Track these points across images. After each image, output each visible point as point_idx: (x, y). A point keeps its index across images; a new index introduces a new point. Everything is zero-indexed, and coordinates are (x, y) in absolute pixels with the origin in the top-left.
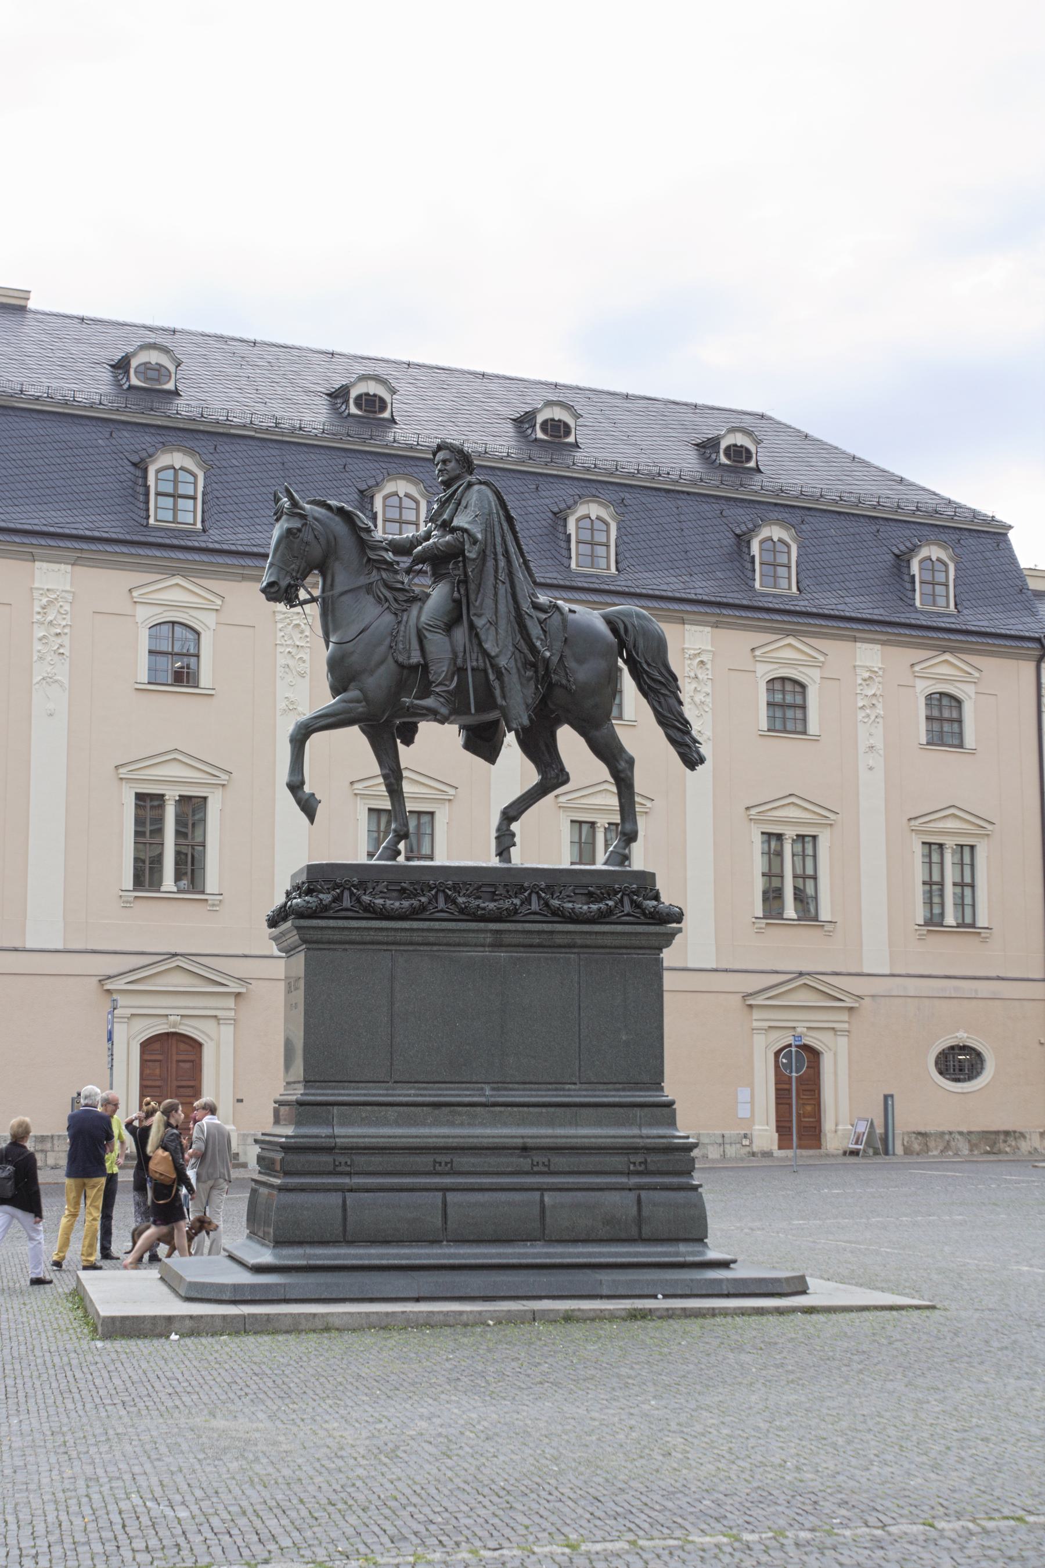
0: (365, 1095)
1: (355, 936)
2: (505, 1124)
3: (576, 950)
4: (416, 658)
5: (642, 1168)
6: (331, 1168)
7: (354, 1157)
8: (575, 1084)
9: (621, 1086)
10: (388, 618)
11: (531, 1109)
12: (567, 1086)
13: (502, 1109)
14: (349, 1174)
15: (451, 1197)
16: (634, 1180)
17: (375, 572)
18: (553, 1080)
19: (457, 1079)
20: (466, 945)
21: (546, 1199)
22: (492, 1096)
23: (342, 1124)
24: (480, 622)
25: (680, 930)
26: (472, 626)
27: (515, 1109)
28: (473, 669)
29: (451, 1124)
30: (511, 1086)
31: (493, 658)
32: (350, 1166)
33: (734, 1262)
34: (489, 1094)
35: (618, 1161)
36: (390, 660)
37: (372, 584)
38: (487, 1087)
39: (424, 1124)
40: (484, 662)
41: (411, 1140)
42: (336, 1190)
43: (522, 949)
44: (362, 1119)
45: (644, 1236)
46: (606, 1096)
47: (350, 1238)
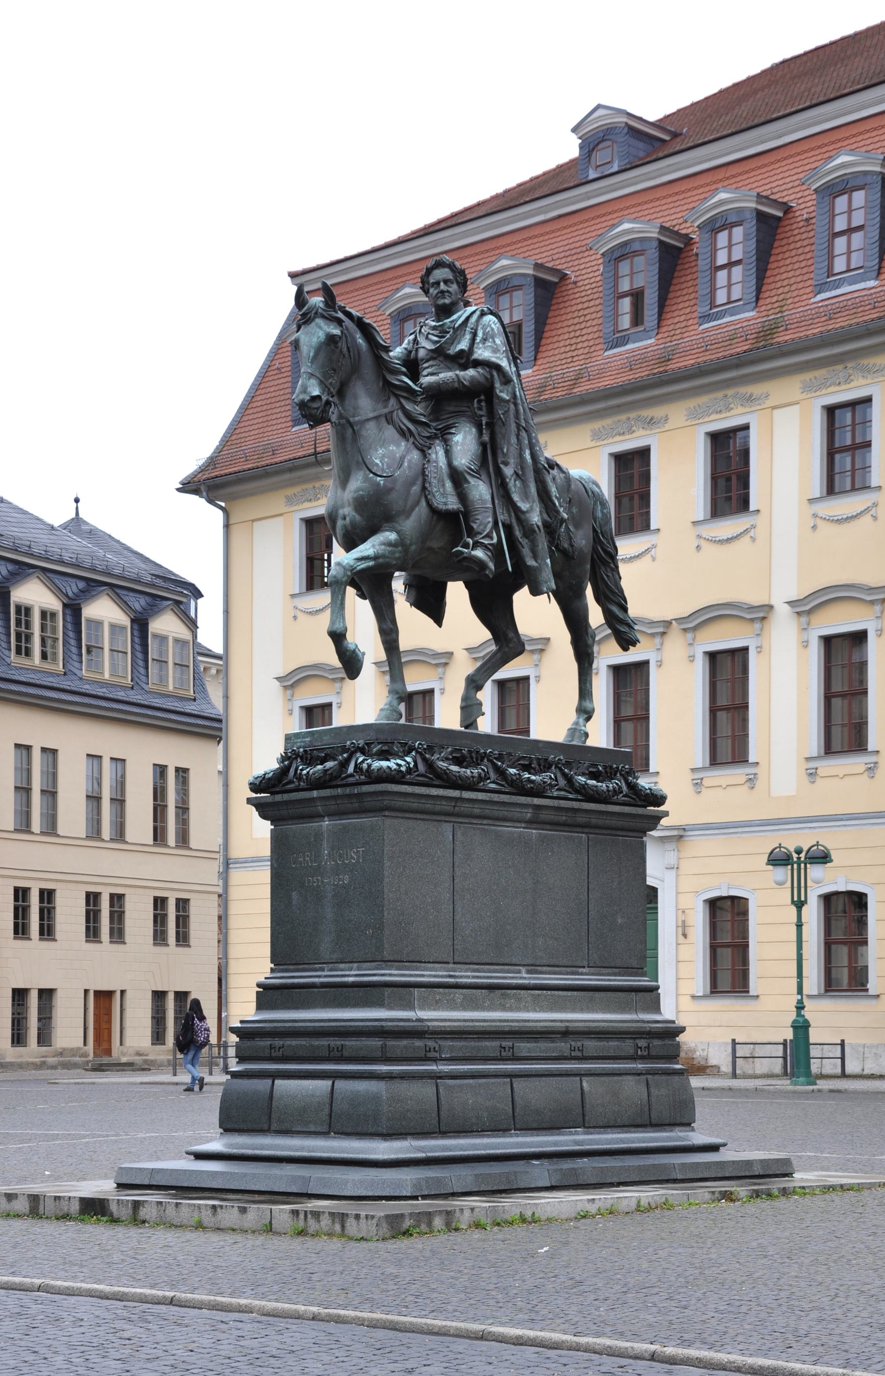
0: (435, 976)
1: (429, 805)
2: (542, 1009)
3: (586, 830)
4: (452, 503)
5: (645, 1053)
6: (422, 1055)
7: (442, 1043)
8: (584, 967)
9: (617, 970)
10: (415, 455)
11: (560, 993)
12: (581, 970)
13: (539, 992)
14: (435, 1060)
15: (517, 1083)
16: (640, 1066)
17: (393, 401)
18: (570, 963)
19: (502, 961)
20: (505, 819)
21: (585, 1084)
22: (530, 978)
23: (422, 1008)
24: (508, 471)
25: (666, 814)
26: (499, 473)
27: (549, 992)
28: (503, 524)
29: (504, 1008)
30: (540, 968)
31: (523, 513)
32: (436, 1051)
33: (724, 1145)
34: (524, 977)
35: (628, 1046)
36: (423, 503)
37: (392, 412)
38: (523, 969)
39: (483, 1009)
40: (510, 516)
41: (402, 1024)
42: (431, 1078)
43: (548, 827)
44: (437, 1002)
45: (653, 1121)
46: (610, 980)
47: (443, 1128)
